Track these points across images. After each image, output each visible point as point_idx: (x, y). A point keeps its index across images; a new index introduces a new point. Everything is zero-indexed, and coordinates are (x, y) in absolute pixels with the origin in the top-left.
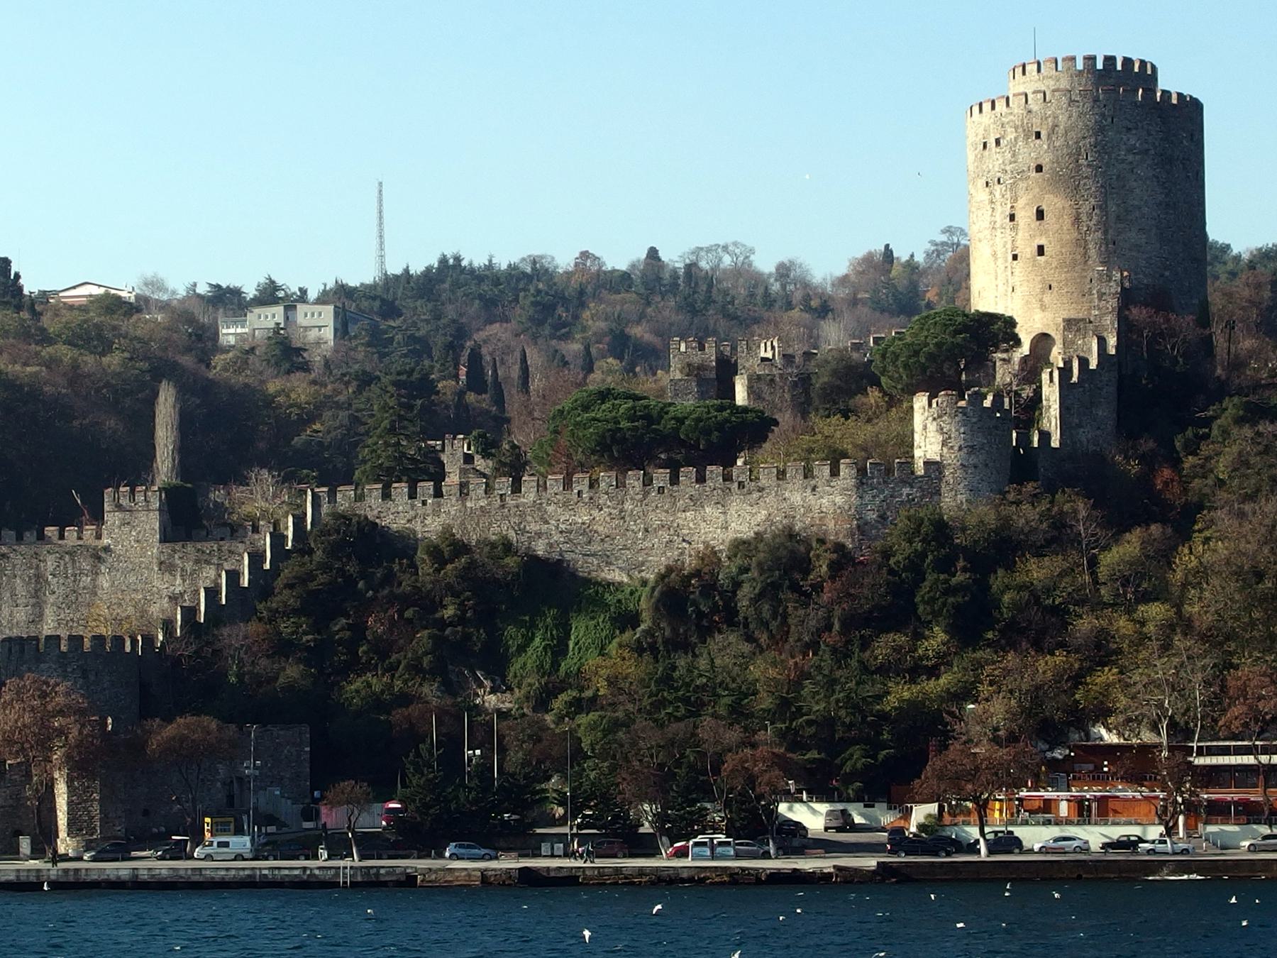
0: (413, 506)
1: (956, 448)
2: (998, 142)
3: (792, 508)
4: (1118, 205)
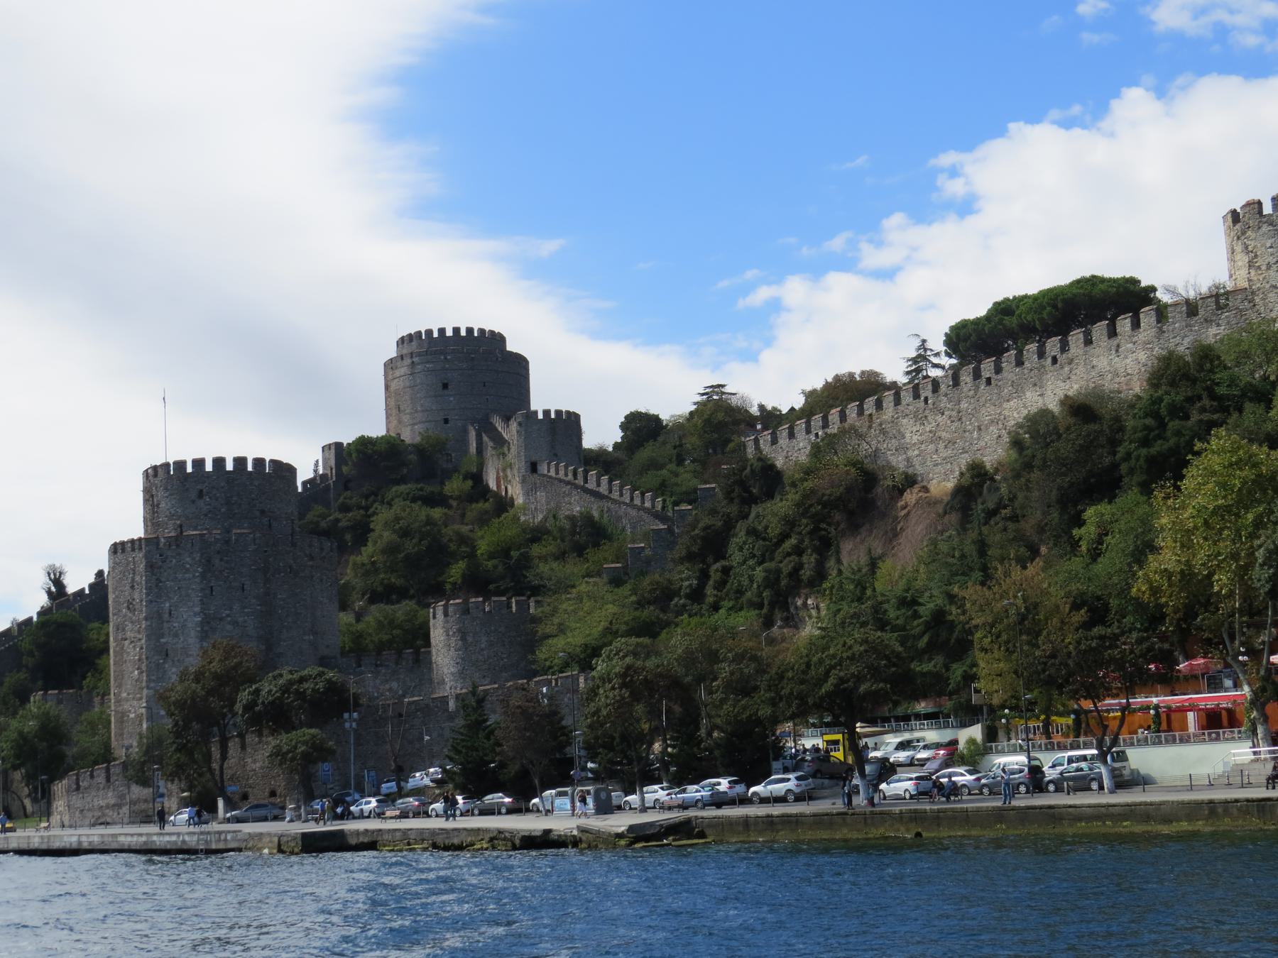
1: (1264, 268)
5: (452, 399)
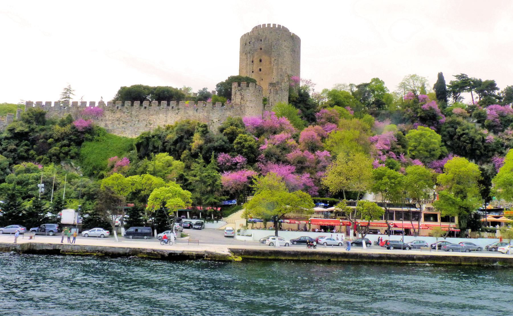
2: (249, 43)
3: (190, 116)
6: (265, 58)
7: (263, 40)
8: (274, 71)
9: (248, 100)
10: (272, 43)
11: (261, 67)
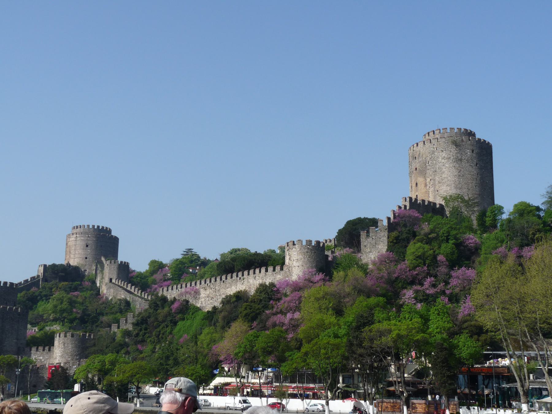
0: (177, 291)
1: (292, 260)
4: (439, 178)
5: (89, 250)
6: (420, 180)
7: (417, 157)
8: (430, 195)
9: (295, 259)
10: (425, 158)
11: (417, 194)
